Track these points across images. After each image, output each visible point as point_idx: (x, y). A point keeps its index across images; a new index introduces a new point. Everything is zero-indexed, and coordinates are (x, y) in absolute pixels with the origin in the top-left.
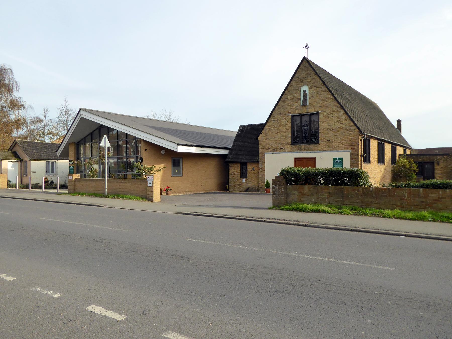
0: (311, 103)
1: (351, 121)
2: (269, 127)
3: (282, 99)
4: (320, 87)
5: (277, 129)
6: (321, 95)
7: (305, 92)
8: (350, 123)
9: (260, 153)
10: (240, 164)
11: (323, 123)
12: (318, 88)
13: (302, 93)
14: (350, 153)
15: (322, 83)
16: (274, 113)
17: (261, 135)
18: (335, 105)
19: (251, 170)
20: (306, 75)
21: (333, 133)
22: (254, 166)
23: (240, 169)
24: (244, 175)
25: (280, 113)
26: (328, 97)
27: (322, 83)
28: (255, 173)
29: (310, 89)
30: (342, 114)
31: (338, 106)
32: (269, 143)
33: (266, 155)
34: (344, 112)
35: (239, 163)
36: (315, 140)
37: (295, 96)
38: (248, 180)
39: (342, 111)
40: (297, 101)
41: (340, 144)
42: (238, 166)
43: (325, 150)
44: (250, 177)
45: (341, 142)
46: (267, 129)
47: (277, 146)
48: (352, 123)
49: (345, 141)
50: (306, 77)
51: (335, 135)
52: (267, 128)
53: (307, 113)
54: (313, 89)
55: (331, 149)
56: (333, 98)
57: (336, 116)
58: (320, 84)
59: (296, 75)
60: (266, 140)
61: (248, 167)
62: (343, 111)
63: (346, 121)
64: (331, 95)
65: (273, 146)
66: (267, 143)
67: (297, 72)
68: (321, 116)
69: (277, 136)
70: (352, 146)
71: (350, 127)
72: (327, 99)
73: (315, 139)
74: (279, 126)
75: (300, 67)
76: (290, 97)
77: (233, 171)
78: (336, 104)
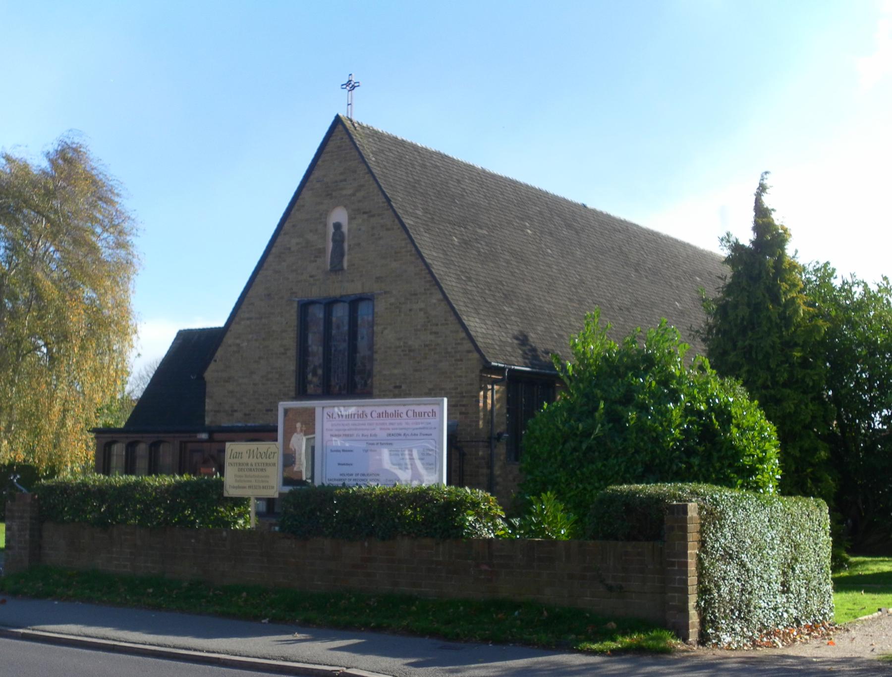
0: (354, 265)
4: (379, 215)
6: (380, 238)
7: (338, 226)
11: (385, 328)
12: (373, 216)
13: (331, 230)
16: (250, 293)
17: (212, 366)
20: (341, 174)
25: (269, 295)
29: (351, 219)
30: (434, 301)
31: (425, 278)
40: (316, 257)
50: (341, 181)
57: (421, 310)
59: (316, 174)
63: (447, 324)
67: (319, 163)
70: (461, 405)
75: (328, 148)
76: (297, 244)
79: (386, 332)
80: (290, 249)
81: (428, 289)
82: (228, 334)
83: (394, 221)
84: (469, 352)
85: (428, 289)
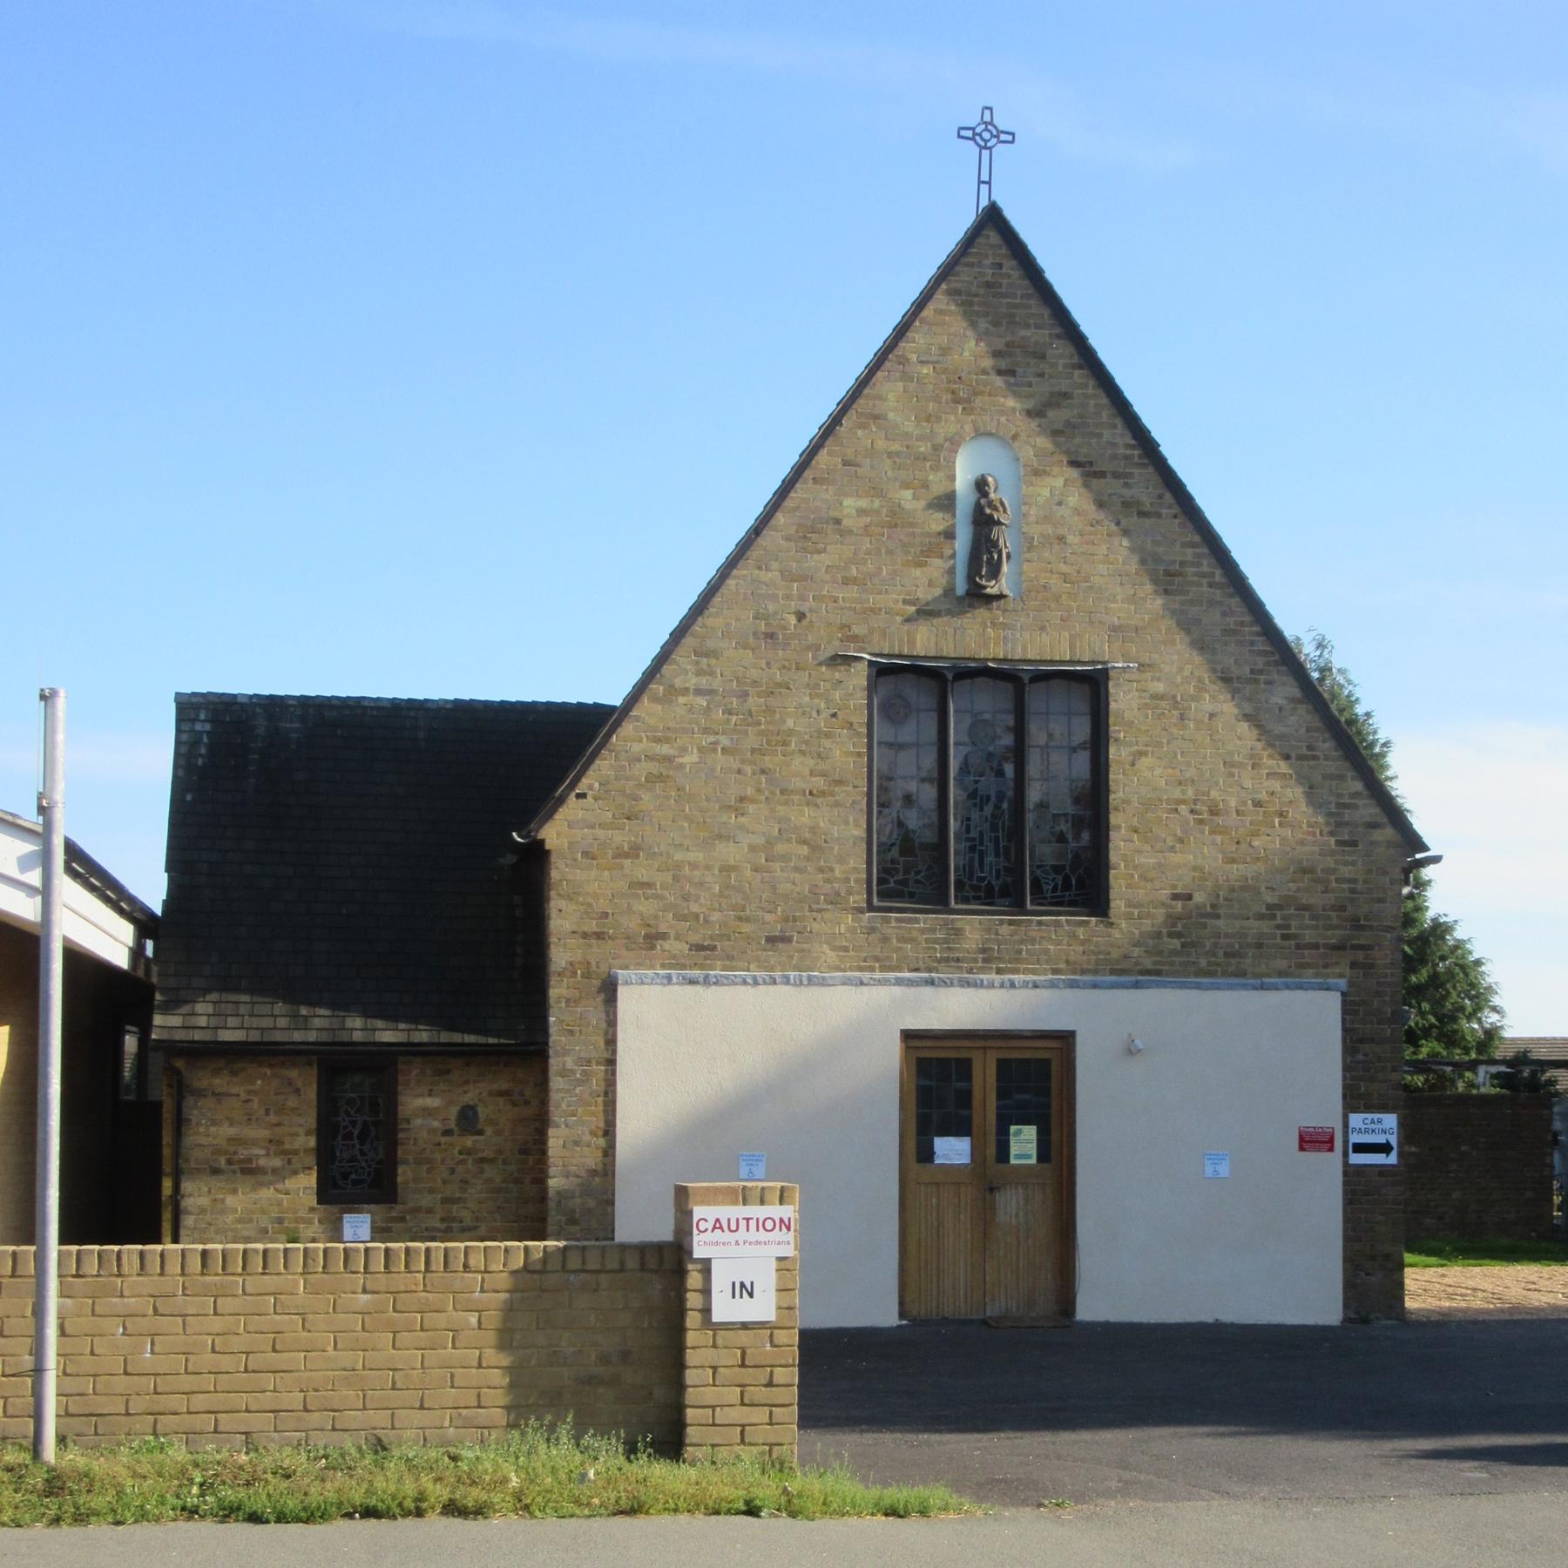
1: (1347, 764)
2: (658, 740)
3: (780, 518)
4: (1116, 475)
5: (739, 772)
8: (1341, 777)
10: (315, 1071)
11: (1142, 754)
12: (1102, 475)
14: (1344, 1003)
15: (1128, 446)
18: (1234, 632)
21: (1219, 839)
22: (478, 1091)
24: (345, 1176)
25: (771, 636)
26: (1182, 563)
27: (1128, 446)
28: (483, 1160)
30: (1281, 702)
31: (1252, 643)
32: (650, 885)
33: (622, 992)
34: (1296, 692)
35: (310, 1064)
36: (1067, 885)
37: (908, 506)
38: (403, 1219)
39: (1284, 684)
41: (1265, 927)
42: (297, 1091)
43: (1158, 973)
44: (431, 1191)
45: (1278, 913)
46: (639, 760)
47: (740, 919)
48: (1353, 778)
49: (1305, 908)
51: (1233, 861)
52: (636, 748)
53: (1005, 660)
54: (1059, 482)
55: (1203, 962)
56: (1218, 576)
58: (1114, 444)
60: (626, 855)
61: (402, 1099)
62: (1290, 680)
63: (1314, 758)
64: (1205, 550)
65: (696, 916)
66: (632, 885)
68: (1123, 701)
69: (741, 828)
70: (1354, 947)
71: (1339, 805)
72: (1168, 573)
73: (1067, 880)
74: (751, 741)
76: (861, 512)
77: (231, 1140)
78: (1242, 624)
79: (1145, 762)
80: (838, 522)
81: (1261, 672)
82: (627, 728)
83: (1160, 497)
84: (1373, 826)
85: (1261, 672)
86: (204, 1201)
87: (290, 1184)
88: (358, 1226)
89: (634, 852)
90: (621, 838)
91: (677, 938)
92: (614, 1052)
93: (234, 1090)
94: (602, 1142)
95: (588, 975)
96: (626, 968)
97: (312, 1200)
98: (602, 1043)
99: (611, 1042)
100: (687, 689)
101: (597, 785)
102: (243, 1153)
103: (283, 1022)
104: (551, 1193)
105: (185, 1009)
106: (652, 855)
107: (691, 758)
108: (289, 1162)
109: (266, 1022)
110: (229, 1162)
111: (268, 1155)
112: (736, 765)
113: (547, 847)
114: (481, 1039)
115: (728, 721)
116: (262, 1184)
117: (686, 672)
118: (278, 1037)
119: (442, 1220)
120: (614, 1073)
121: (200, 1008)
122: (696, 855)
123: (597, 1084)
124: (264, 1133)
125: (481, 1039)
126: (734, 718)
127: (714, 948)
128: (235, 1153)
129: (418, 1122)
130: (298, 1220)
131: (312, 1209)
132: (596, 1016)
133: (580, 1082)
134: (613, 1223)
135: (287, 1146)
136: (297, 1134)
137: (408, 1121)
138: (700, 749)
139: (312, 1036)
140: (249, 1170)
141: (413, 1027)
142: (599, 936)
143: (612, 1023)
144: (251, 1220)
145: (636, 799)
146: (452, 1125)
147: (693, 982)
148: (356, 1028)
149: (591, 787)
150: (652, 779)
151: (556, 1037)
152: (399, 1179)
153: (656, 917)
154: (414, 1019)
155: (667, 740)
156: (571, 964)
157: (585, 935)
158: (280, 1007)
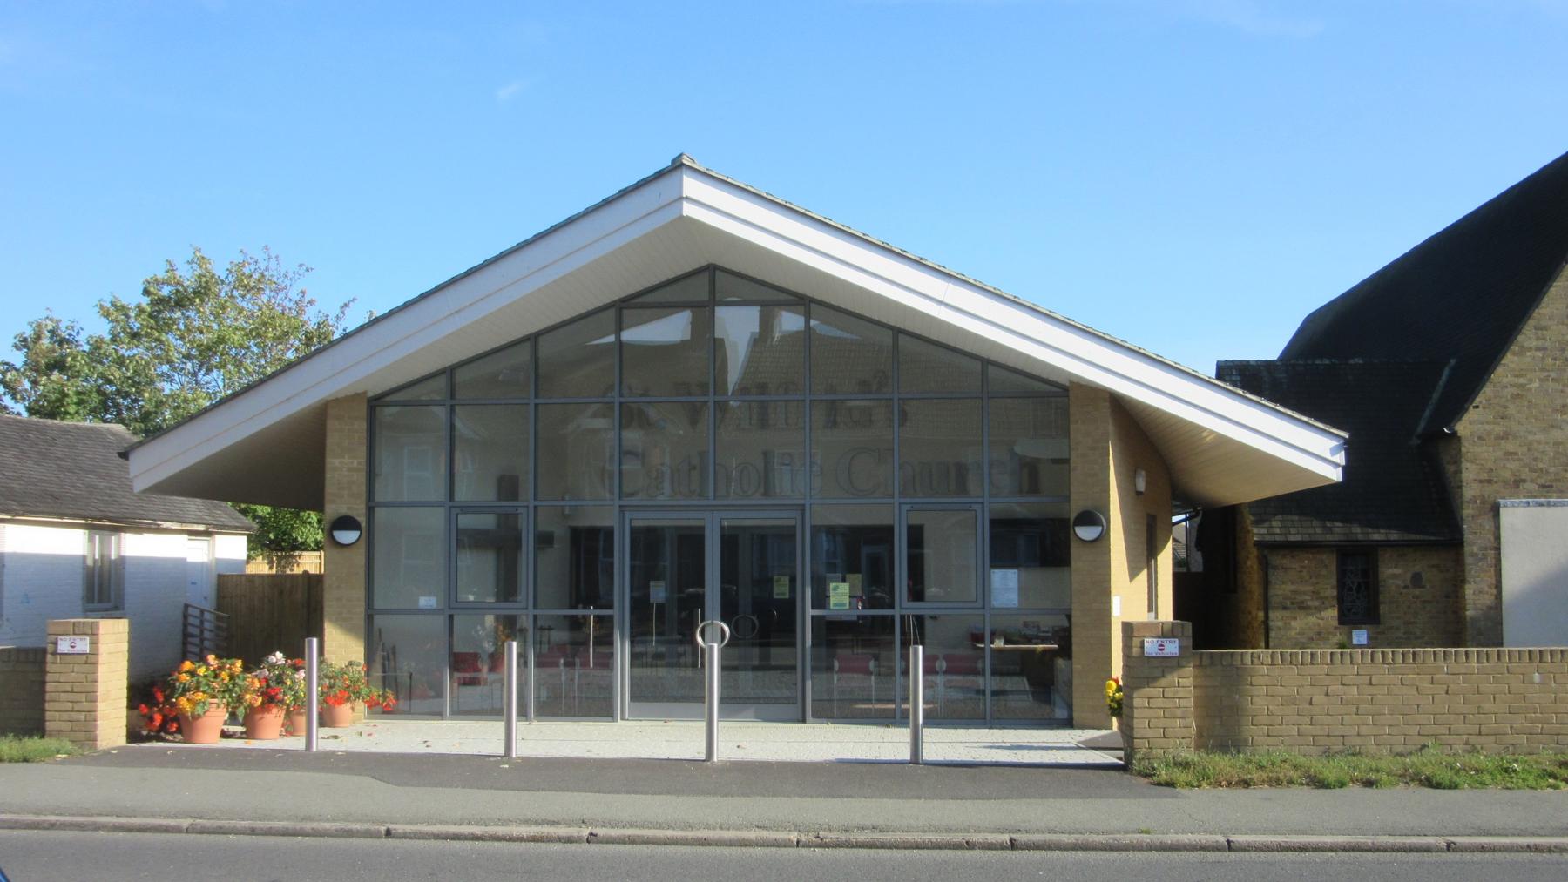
2: (1517, 376)
5: (1562, 391)
9: (1468, 502)
10: (1335, 556)
19: (1399, 582)
23: (1334, 581)
28: (1424, 602)
32: (1516, 454)
33: (1502, 510)
38: (1384, 633)
42: (1326, 566)
46: (1506, 387)
52: (1505, 380)
60: (1502, 438)
65: (1541, 470)
77: (1294, 592)
86: (1280, 624)
87: (1324, 614)
88: (1360, 636)
89: (1506, 436)
90: (1498, 429)
91: (1532, 481)
92: (1499, 543)
93: (1294, 566)
94: (1494, 591)
95: (1483, 502)
96: (1504, 498)
97: (1335, 623)
98: (1492, 539)
99: (1498, 538)
100: (1531, 348)
101: (1484, 401)
102: (1299, 598)
103: (1318, 530)
104: (1468, 619)
105: (1267, 524)
106: (1515, 437)
107: (1536, 384)
108: (1323, 603)
109: (1311, 531)
110: (1292, 603)
111: (1312, 600)
112: (1560, 387)
113: (1459, 435)
114: (1426, 538)
115: (1555, 364)
116: (1309, 615)
117: (1530, 338)
118: (1319, 538)
119: (1405, 633)
120: (1500, 554)
121: (1274, 523)
122: (1539, 437)
123: (1491, 560)
124: (1311, 588)
125: (1426, 538)
126: (1557, 362)
127: (1551, 487)
128: (1295, 599)
129: (1391, 581)
130: (1329, 633)
131: (1336, 628)
132: (1488, 524)
133: (1481, 560)
134: (1502, 634)
135: (1322, 595)
136: (1327, 589)
137: (1385, 581)
138: (1541, 380)
139: (1336, 537)
140: (1302, 607)
141: (1387, 531)
142: (1489, 481)
143: (1498, 528)
144: (1304, 634)
145: (1506, 407)
146: (1408, 583)
147: (1541, 505)
148: (1358, 532)
149: (1481, 402)
150: (1515, 397)
151: (1468, 537)
152: (1381, 612)
153: (1519, 471)
154: (1389, 527)
155: (1521, 376)
156: (1474, 497)
157: (1481, 481)
158: (1315, 523)
